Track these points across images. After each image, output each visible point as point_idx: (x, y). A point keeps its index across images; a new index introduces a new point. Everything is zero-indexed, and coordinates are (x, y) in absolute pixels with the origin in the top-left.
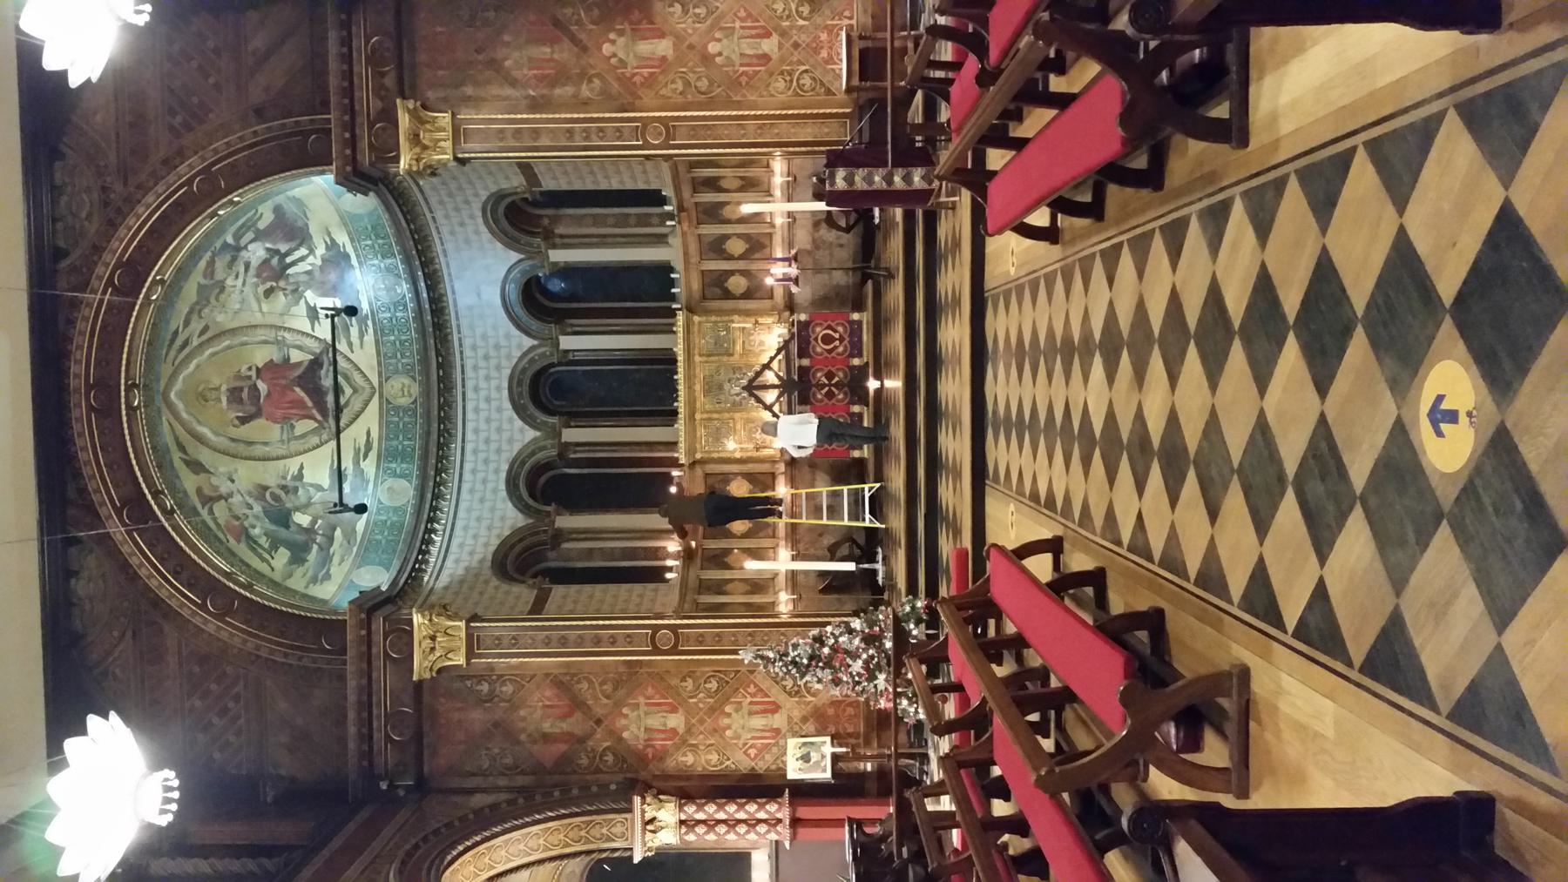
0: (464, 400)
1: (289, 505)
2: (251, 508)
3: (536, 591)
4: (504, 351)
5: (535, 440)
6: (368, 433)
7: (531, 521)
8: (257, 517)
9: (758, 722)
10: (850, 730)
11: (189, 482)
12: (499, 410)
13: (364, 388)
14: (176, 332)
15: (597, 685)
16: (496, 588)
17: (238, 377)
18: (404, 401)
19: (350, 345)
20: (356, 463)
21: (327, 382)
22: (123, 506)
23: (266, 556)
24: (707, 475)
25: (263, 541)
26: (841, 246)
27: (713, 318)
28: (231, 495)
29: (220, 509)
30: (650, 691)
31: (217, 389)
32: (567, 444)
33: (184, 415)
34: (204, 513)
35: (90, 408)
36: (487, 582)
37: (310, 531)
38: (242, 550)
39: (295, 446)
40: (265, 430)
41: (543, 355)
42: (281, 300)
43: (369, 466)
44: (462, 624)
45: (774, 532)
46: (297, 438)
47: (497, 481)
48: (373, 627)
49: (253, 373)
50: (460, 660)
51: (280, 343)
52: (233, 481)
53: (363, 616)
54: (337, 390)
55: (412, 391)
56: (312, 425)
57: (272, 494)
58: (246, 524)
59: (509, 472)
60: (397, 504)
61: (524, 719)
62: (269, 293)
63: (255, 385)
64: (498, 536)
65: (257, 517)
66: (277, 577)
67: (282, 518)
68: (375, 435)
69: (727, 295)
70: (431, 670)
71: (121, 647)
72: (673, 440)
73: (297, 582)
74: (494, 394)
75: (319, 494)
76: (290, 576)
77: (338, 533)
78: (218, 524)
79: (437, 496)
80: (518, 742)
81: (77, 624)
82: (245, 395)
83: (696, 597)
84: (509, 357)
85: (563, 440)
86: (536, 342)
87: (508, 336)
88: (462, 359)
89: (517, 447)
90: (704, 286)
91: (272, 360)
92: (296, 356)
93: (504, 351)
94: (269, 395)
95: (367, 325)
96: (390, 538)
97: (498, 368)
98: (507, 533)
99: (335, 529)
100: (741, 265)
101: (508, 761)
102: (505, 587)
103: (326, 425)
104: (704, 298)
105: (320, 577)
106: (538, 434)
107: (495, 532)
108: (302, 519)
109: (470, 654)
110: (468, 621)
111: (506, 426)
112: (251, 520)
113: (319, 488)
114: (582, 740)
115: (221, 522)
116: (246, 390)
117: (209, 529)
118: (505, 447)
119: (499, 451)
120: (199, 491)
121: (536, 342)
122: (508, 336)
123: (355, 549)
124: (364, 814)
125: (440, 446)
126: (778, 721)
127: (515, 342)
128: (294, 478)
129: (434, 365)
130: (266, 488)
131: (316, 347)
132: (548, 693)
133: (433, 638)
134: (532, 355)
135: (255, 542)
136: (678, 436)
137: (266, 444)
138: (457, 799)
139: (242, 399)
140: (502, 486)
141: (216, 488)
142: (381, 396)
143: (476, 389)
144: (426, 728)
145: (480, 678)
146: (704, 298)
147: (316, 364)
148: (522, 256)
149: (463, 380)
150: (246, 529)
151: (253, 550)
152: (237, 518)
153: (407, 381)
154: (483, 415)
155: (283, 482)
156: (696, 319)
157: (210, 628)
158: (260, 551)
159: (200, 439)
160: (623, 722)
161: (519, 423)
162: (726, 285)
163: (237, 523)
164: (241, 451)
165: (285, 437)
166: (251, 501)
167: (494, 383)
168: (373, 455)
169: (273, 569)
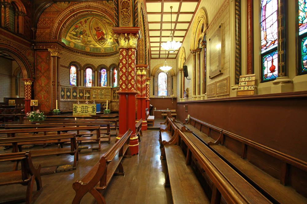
2: (82, 29)
5: (95, 67)
6: (96, 46)
9: (43, 96)
10: (42, 109)
11: (83, 20)
14: (102, 19)
16: (69, 61)
17: (101, 28)
18: (101, 51)
20: (92, 44)
21: (103, 41)
24: (90, 90)
25: (76, 31)
29: (80, 25)
30: (47, 81)
31: (98, 25)
34: (78, 22)
35: (87, 5)
36: (70, 60)
37: (80, 37)
38: (73, 27)
39: (93, 36)
42: (111, 34)
43: (92, 46)
51: (106, 34)
52: (85, 27)
54: (102, 42)
56: (97, 38)
59: (91, 64)
60: (86, 49)
62: (111, 32)
65: (80, 30)
66: (69, 32)
67: (81, 33)
68: (96, 47)
73: (69, 34)
78: (77, 24)
79: (87, 54)
80: (41, 63)
81: (58, 3)
82: (98, 29)
84: (107, 64)
92: (105, 36)
94: (99, 33)
98: (81, 64)
101: (38, 62)
104: (113, 90)
108: (82, 36)
109: (52, 56)
111: (98, 64)
112: (79, 29)
113: (87, 39)
114: (41, 72)
117: (75, 23)
118: (95, 64)
126: (43, 99)
135: (76, 29)
139: (98, 28)
143: (103, 60)
144: (43, 51)
150: (78, 28)
152: (79, 27)
154: (105, 61)
161: (98, 65)
164: (90, 29)
167: (103, 62)
168: (93, 46)
169: (71, 31)
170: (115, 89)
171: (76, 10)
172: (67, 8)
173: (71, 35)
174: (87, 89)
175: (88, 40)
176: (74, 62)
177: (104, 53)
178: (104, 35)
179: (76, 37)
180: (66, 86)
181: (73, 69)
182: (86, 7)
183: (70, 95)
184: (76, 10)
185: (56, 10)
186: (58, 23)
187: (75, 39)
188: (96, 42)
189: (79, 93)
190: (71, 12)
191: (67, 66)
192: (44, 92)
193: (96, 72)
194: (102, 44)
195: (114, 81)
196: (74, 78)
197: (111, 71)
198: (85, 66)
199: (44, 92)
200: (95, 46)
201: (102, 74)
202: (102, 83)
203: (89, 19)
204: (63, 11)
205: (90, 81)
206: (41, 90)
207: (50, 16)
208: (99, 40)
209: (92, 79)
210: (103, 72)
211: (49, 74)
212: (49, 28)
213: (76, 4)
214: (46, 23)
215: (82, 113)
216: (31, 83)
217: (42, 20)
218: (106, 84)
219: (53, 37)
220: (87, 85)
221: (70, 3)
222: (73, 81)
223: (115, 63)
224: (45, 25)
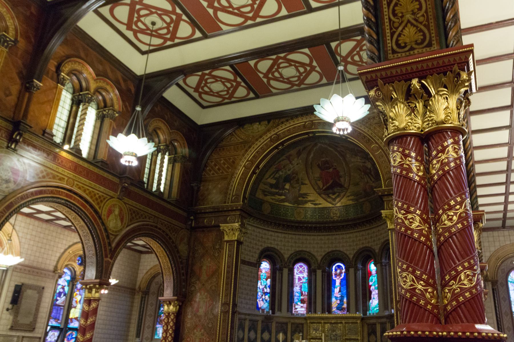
0: (332, 235)
1: (292, 182)
3: (255, 262)
5: (317, 260)
6: (320, 204)
7: (286, 260)
8: (286, 173)
11: (293, 152)
12: (329, 247)
13: (335, 201)
15: (214, 284)
19: (349, 196)
20: (310, 201)
21: (336, 190)
22: (278, 135)
23: (272, 176)
25: (277, 175)
28: (292, 164)
29: (287, 162)
33: (315, 149)
34: (284, 157)
35: (306, 122)
36: (261, 246)
37: (283, 188)
38: (273, 169)
40: (317, 173)
43: (309, 205)
44: (236, 238)
46: (316, 182)
48: (237, 211)
49: (334, 167)
50: (226, 238)
52: (297, 164)
53: (239, 208)
54: (334, 194)
55: (335, 217)
57: (295, 177)
58: (283, 170)
61: (207, 260)
63: (331, 168)
64: (281, 249)
65: (286, 173)
67: (287, 179)
68: (320, 206)
69: (369, 335)
70: (223, 230)
71: (239, 139)
75: (298, 191)
76: (265, 184)
77: (283, 197)
78: (280, 161)
81: (245, 127)
82: (327, 165)
83: (248, 320)
86: (351, 260)
88: (346, 234)
91: (339, 172)
92: (342, 180)
95: (355, 201)
96: (282, 213)
98: (282, 252)
99: (285, 196)
101: (196, 255)
102: (258, 252)
103: (322, 191)
104: (368, 325)
105: (266, 193)
107: (283, 247)
108: (287, 186)
109: (227, 241)
110: (237, 240)
113: (299, 190)
114: (199, 279)
115: (282, 163)
116: (328, 165)
120: (290, 155)
121: (351, 260)
123: (278, 203)
124: (180, 212)
125: (315, 227)
128: (302, 182)
129: (343, 224)
130: (297, 174)
131: (346, 185)
132: (214, 267)
133: (232, 230)
135: (277, 173)
137: (312, 173)
138: (186, 240)
140: (300, 249)
141: (293, 160)
142: (333, 207)
145: (220, 245)
147: (341, 186)
149: (339, 234)
150: (281, 170)
151: (273, 173)
152: (284, 167)
153: (338, 215)
155: (300, 179)
156: (359, 322)
157: (241, 163)
158: (273, 175)
159: (309, 153)
160: (203, 293)
161: (324, 254)
163: (282, 167)
165: (316, 178)
166: (291, 170)
168: (313, 206)
169: (267, 179)
170: (372, 321)
171: (282, 136)
172: (265, 133)
173: (266, 187)
174: (297, 321)
175: (301, 192)
176: (267, 249)
177: (337, 222)
178: (341, 177)
179: (276, 188)
180: (249, 315)
181: (265, 266)
182: (304, 127)
184: (282, 136)
185: (241, 141)
186: (244, 166)
187: (273, 194)
188: (320, 194)
189: (276, 332)
190: (272, 141)
191: (253, 260)
192: (202, 330)
193: (319, 273)
194: (334, 200)
195: (367, 295)
196: (265, 291)
197: (360, 266)
198: (292, 259)
199: (202, 330)
200: (315, 204)
202: (335, 303)
203: (307, 147)
204: (257, 140)
205: (302, 297)
206: (196, 327)
207: (228, 153)
208: (328, 189)
209: (307, 290)
210: (336, 270)
211: (217, 284)
212: (225, 178)
213: (282, 123)
214: (219, 169)
216: (178, 307)
217: (213, 163)
218: (345, 306)
219: (233, 196)
220: (296, 309)
221: (271, 122)
222: (263, 300)
223: (370, 245)
224: (217, 173)
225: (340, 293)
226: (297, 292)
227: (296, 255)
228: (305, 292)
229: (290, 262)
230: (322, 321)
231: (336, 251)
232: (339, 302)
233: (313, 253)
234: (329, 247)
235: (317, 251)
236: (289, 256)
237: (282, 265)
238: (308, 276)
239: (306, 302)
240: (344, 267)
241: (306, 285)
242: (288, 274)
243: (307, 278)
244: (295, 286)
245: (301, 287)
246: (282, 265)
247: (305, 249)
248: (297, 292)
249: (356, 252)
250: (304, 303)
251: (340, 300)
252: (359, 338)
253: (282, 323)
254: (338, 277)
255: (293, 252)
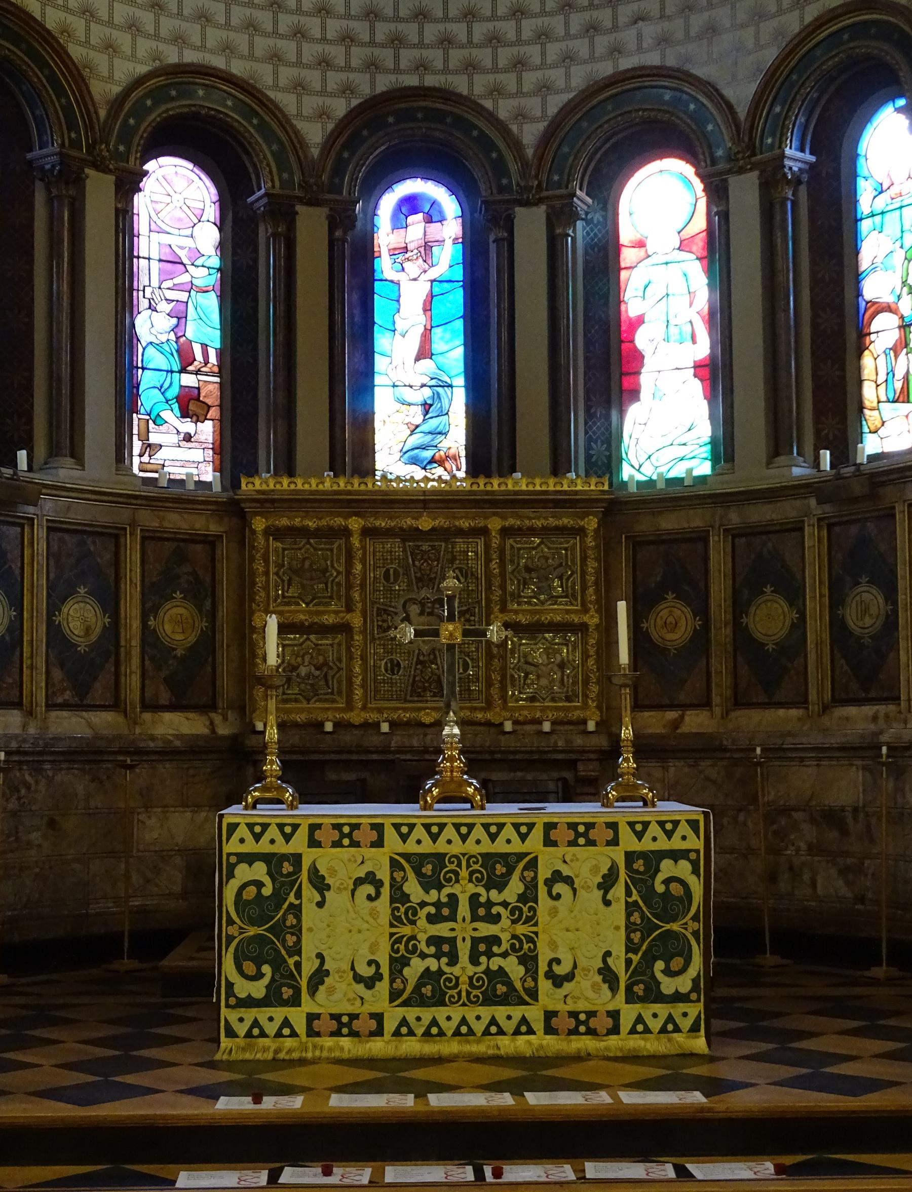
4: (509, 81)
5: (298, 142)
7: (102, 113)
12: (372, 66)
26: (773, 878)
27: (592, 565)
32: (290, 219)
41: (500, 168)
45: (65, 706)
47: (203, 47)
72: (299, 468)
74: (408, 56)
84: (496, 91)
85: (299, 208)
86: (530, 152)
87: (544, 89)
89: (287, 102)
90: (662, 540)
93: (509, 81)
97: (471, 67)
98: (76, 51)
100: (722, 634)
104: (637, 544)
106: (315, 152)
107: (78, 25)
118: (287, 74)
119: (275, 58)
121: (530, 152)
122: (544, 89)
127: (533, 105)
134: (502, 145)
136: (307, 476)
140: (191, 57)
146: (637, 544)
148: (742, 112)
156: (591, 523)
161: (340, 108)
162: (670, 596)
167: (436, 57)
170: (670, 523)
174: (175, 521)
183: (54, 608)
201: (385, 266)
205: (189, 380)
209: (214, 339)
215: (417, 1000)
220: (150, 448)
225: (426, 363)
226: (158, 346)
227: (159, 95)
228: (204, 347)
229: (126, 135)
230: (355, 524)
231: (422, 92)
232: (418, 419)
233: (271, 94)
234: (372, 66)
235: (299, 87)
236: (116, 89)
237: (75, 144)
238: (221, 246)
239: (214, 413)
240: (450, 205)
241: (211, 304)
242: (117, 210)
243: (215, 262)
244: (144, 304)
245: (180, 317)
246: (75, 144)
247: (218, 62)
248: (158, 346)
249: (567, 110)
250: (198, 418)
251: (427, 407)
252: (593, 619)
253: (81, 532)
254: (413, 268)
255: (142, 69)
